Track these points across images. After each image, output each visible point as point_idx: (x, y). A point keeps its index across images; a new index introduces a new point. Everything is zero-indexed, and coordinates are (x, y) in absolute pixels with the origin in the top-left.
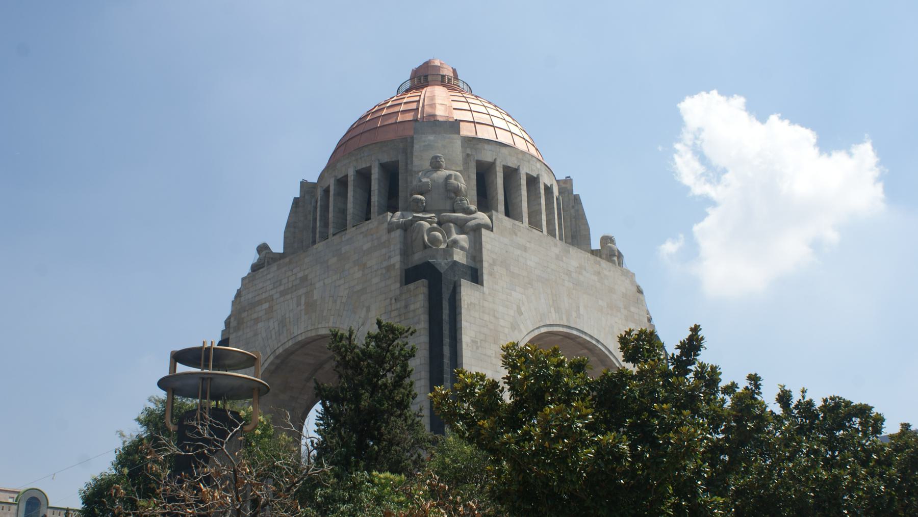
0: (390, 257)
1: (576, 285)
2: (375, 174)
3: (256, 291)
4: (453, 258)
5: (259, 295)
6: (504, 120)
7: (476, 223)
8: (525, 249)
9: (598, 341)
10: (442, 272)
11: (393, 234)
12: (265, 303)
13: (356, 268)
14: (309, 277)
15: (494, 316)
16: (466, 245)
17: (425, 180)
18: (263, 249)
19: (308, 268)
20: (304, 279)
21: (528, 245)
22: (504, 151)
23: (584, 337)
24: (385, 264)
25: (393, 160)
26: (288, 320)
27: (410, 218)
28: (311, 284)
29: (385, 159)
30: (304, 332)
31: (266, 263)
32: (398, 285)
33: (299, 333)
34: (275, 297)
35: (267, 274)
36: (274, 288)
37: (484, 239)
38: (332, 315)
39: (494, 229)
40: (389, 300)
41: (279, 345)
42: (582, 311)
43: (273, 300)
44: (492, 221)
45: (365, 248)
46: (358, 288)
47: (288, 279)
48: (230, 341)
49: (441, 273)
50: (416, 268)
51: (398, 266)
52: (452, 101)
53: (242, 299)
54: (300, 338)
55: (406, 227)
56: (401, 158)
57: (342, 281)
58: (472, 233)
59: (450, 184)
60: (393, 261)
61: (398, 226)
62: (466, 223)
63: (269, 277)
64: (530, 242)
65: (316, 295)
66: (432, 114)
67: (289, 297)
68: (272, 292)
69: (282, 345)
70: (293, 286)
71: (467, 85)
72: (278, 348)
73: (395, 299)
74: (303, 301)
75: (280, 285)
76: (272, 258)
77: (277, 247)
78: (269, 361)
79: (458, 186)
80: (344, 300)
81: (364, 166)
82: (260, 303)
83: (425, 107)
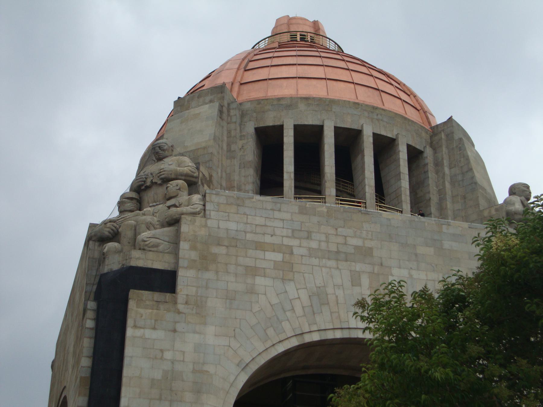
3: (247, 223)
5: (255, 233)
14: (375, 253)
19: (371, 240)
26: (332, 298)
28: (381, 265)
29: (410, 143)
34: (295, 251)
35: (273, 210)
36: (293, 237)
41: (315, 328)
43: (292, 253)
53: (210, 223)
56: (428, 153)
63: (277, 214)
67: (332, 263)
68: (286, 241)
70: (338, 252)
75: (309, 238)
81: (383, 133)
82: (260, 246)
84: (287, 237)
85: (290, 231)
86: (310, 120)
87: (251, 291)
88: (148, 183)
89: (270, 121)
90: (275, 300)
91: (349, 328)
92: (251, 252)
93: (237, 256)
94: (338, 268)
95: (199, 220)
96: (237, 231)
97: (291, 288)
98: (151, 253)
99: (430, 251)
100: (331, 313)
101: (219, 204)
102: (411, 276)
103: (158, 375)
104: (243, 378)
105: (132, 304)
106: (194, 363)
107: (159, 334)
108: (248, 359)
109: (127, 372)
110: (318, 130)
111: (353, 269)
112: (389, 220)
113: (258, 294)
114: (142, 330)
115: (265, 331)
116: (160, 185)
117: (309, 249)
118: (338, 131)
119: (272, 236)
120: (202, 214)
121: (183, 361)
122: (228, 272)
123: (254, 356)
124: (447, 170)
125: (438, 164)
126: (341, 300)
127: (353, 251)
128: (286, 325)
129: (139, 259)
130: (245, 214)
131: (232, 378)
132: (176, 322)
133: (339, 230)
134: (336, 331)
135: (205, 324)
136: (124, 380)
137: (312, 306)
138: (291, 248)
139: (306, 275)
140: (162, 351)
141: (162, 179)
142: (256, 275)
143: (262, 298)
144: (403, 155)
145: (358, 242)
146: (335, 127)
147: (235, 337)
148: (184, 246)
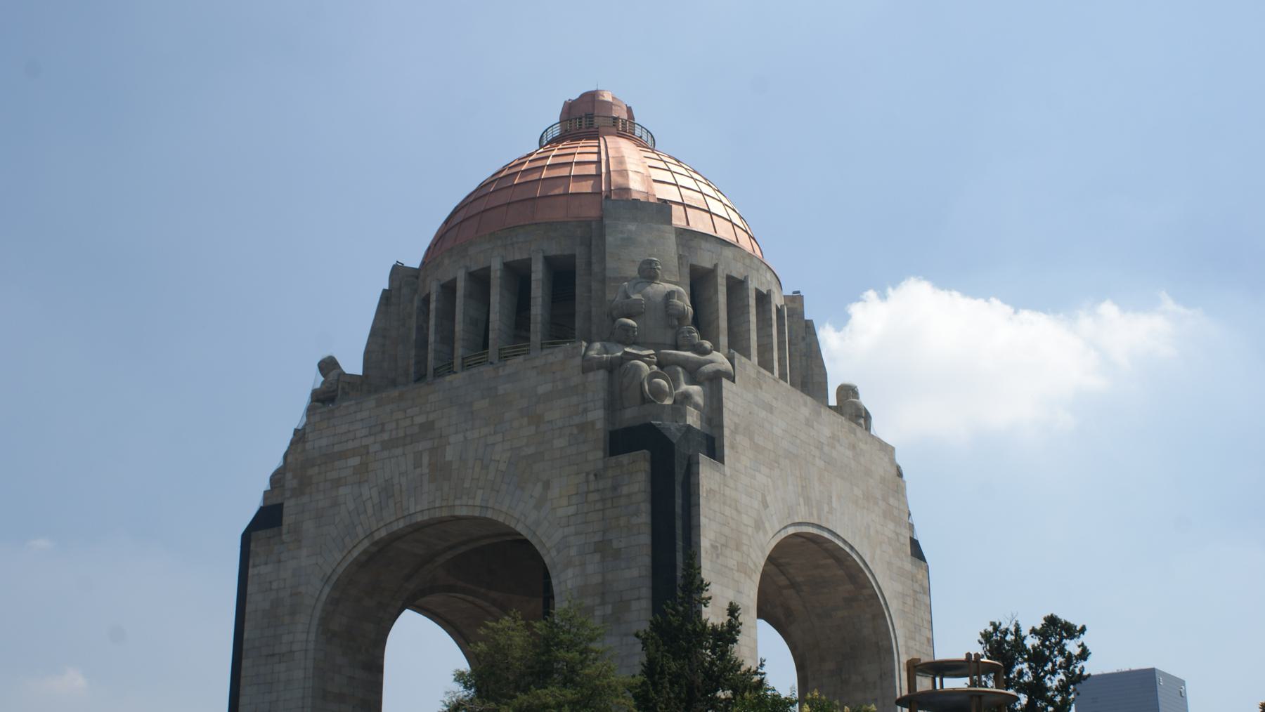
0: (585, 411)
1: (829, 464)
2: (538, 274)
3: (335, 435)
4: (686, 421)
5: (341, 443)
6: (722, 202)
7: (714, 369)
8: (770, 409)
9: (852, 548)
10: (675, 441)
11: (591, 376)
12: (354, 456)
15: (737, 510)
16: (700, 400)
17: (636, 297)
18: (328, 366)
19: (435, 411)
20: (428, 426)
21: (774, 403)
22: (728, 252)
23: (837, 541)
25: (566, 253)
27: (619, 354)
28: (441, 436)
29: (554, 250)
30: (428, 509)
31: (339, 392)
32: (600, 454)
33: (419, 508)
34: (371, 450)
35: (355, 412)
36: (370, 435)
37: (725, 393)
38: (480, 488)
39: (737, 379)
40: (584, 474)
41: (382, 524)
42: (835, 504)
43: (368, 453)
44: (733, 366)
45: (541, 390)
46: (531, 450)
48: (285, 510)
49: (672, 444)
50: (629, 431)
51: (599, 425)
52: (649, 167)
53: (308, 446)
54: (419, 518)
55: (614, 368)
56: (579, 252)
58: (707, 383)
59: (673, 305)
60: (591, 416)
61: (601, 365)
62: (700, 367)
63: (359, 416)
64: (776, 399)
65: (450, 454)
66: (624, 186)
67: (399, 451)
68: (365, 441)
69: (385, 525)
71: (648, 131)
72: (378, 529)
73: (595, 475)
74: (425, 460)
75: (383, 431)
76: (349, 383)
77: (353, 365)
78: (361, 548)
79: (685, 309)
81: (518, 257)
82: (343, 455)
83: (612, 173)
94: (404, 454)
96: (327, 446)
100: (395, 504)
102: (465, 438)
104: (327, 590)
108: (329, 571)
115: (343, 540)
119: (353, 440)
123: (334, 567)
133: (408, 411)
137: (380, 502)
138: (367, 446)
140: (270, 582)
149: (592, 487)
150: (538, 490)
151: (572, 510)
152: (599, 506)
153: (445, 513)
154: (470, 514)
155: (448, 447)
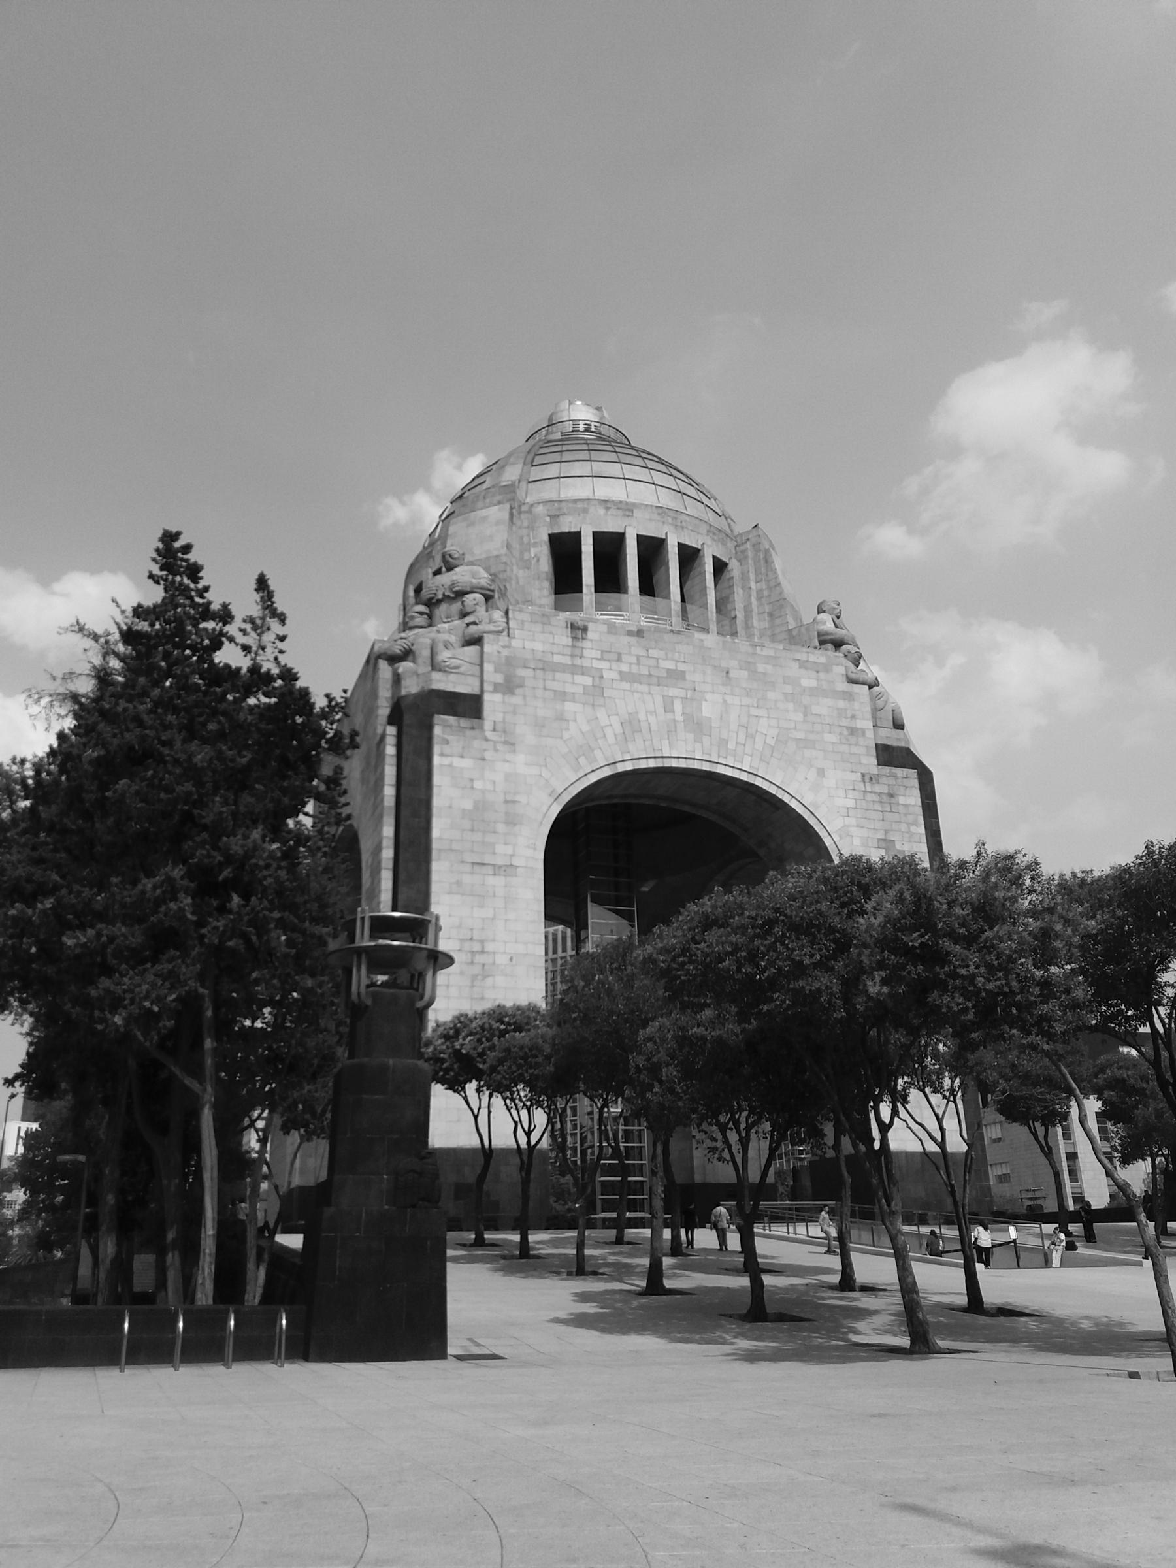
0: (853, 717)
3: (554, 644)
11: (856, 688)
12: (583, 674)
13: (791, 706)
24: (845, 723)
26: (644, 725)
34: (605, 676)
36: (602, 659)
43: (602, 677)
45: (805, 683)
47: (638, 659)
51: (870, 734)
53: (514, 643)
54: (674, 764)
56: (734, 565)
57: (762, 712)
60: (860, 724)
67: (644, 688)
68: (596, 664)
70: (650, 675)
75: (619, 660)
80: (772, 742)
84: (597, 659)
85: (599, 652)
86: (611, 525)
87: (561, 717)
88: (440, 597)
89: (567, 525)
90: (585, 728)
91: (662, 757)
92: (558, 675)
93: (544, 680)
94: (650, 693)
95: (503, 638)
97: (601, 714)
98: (452, 675)
99: (745, 674)
101: (523, 622)
102: (725, 701)
103: (468, 805)
105: (437, 730)
106: (505, 793)
107: (466, 763)
109: (437, 802)
110: (620, 538)
111: (666, 694)
112: (702, 640)
113: (568, 721)
114: (449, 758)
116: (453, 599)
117: (621, 672)
118: (641, 539)
120: (505, 633)
121: (494, 791)
122: (535, 697)
124: (753, 585)
125: (744, 577)
126: (654, 727)
127: (665, 675)
128: (598, 753)
129: (440, 681)
130: (551, 633)
131: (545, 809)
132: (485, 750)
133: (650, 651)
134: (649, 760)
135: (514, 751)
136: (435, 811)
139: (617, 701)
140: (472, 780)
141: (454, 592)
142: (564, 701)
143: (572, 725)
144: (709, 568)
145: (670, 665)
146: (638, 535)
147: (546, 766)
148: (488, 667)
149: (869, 789)
150: (812, 775)
151: (851, 803)
152: (878, 807)
153: (706, 767)
154: (736, 774)
155: (704, 703)
